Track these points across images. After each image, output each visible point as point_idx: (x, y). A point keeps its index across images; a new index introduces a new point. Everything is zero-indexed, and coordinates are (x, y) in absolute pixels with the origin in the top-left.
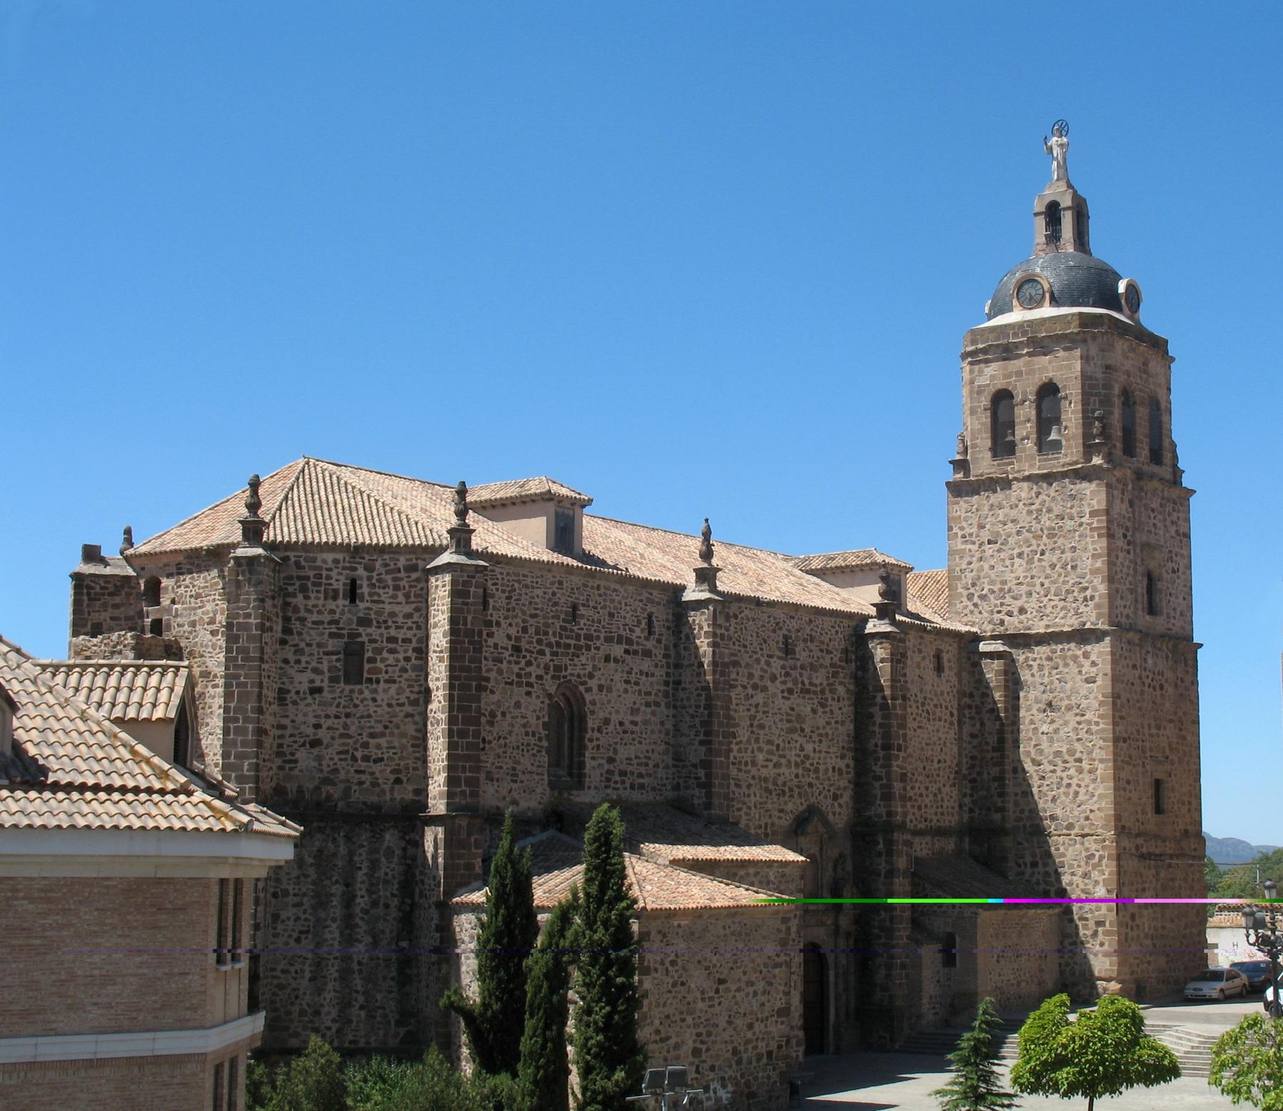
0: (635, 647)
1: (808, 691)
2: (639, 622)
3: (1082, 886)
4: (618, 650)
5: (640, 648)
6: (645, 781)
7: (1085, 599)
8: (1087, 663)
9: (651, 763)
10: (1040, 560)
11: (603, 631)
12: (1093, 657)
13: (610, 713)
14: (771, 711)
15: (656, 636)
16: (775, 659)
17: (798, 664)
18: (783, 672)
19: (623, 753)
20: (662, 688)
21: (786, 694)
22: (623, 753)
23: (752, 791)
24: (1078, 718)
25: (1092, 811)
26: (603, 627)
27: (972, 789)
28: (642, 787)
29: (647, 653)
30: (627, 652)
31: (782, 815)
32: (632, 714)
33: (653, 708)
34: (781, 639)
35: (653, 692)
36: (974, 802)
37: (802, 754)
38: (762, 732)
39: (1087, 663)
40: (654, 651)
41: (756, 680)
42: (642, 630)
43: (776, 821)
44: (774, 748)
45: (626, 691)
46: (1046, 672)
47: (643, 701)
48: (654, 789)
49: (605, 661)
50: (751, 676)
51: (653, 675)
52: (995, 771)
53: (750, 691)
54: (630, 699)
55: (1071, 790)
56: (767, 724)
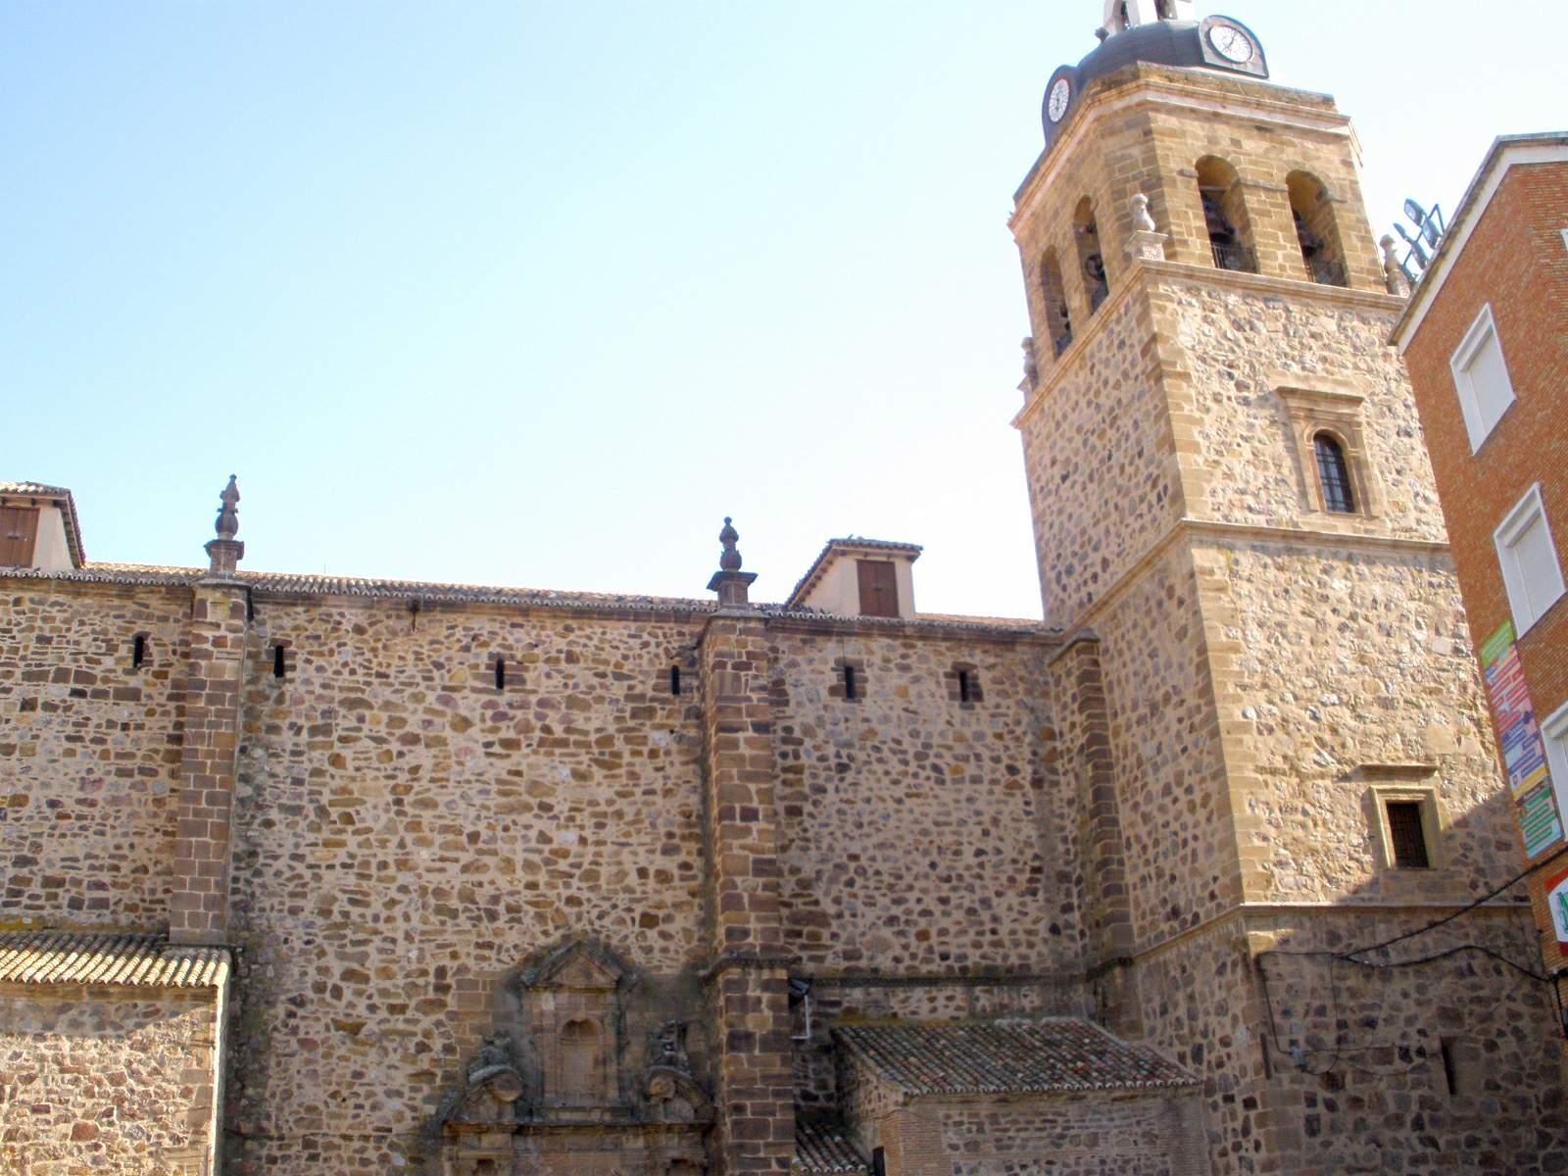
0: (99, 685)
1: (563, 743)
2: (112, 649)
3: (1219, 1035)
4: (57, 692)
5: (111, 687)
6: (112, 894)
7: (1160, 499)
8: (1170, 606)
9: (126, 867)
10: (1109, 470)
11: (22, 664)
12: (1179, 591)
13: (28, 788)
14: (453, 778)
15: (155, 667)
16: (466, 692)
17: (533, 699)
18: (489, 713)
19: (53, 852)
20: (165, 746)
21: (497, 749)
22: (53, 852)
23: (397, 911)
24: (1182, 712)
25: (1215, 879)
26: (23, 658)
27: (1080, 895)
28: (102, 904)
29: (134, 695)
30: (75, 693)
31: (486, 953)
32: (82, 789)
33: (138, 778)
34: (484, 659)
35: (140, 754)
36: (1083, 917)
37: (546, 848)
38: (427, 816)
39: (1170, 606)
40: (145, 690)
41: (413, 726)
42: (119, 661)
43: (471, 963)
44: (464, 839)
45: (70, 753)
46: (1135, 649)
47: (113, 768)
48: (132, 908)
49: (23, 708)
50: (396, 722)
51: (140, 727)
52: (1097, 853)
53: (395, 746)
54: (78, 765)
55: (1188, 850)
56: (442, 800)
